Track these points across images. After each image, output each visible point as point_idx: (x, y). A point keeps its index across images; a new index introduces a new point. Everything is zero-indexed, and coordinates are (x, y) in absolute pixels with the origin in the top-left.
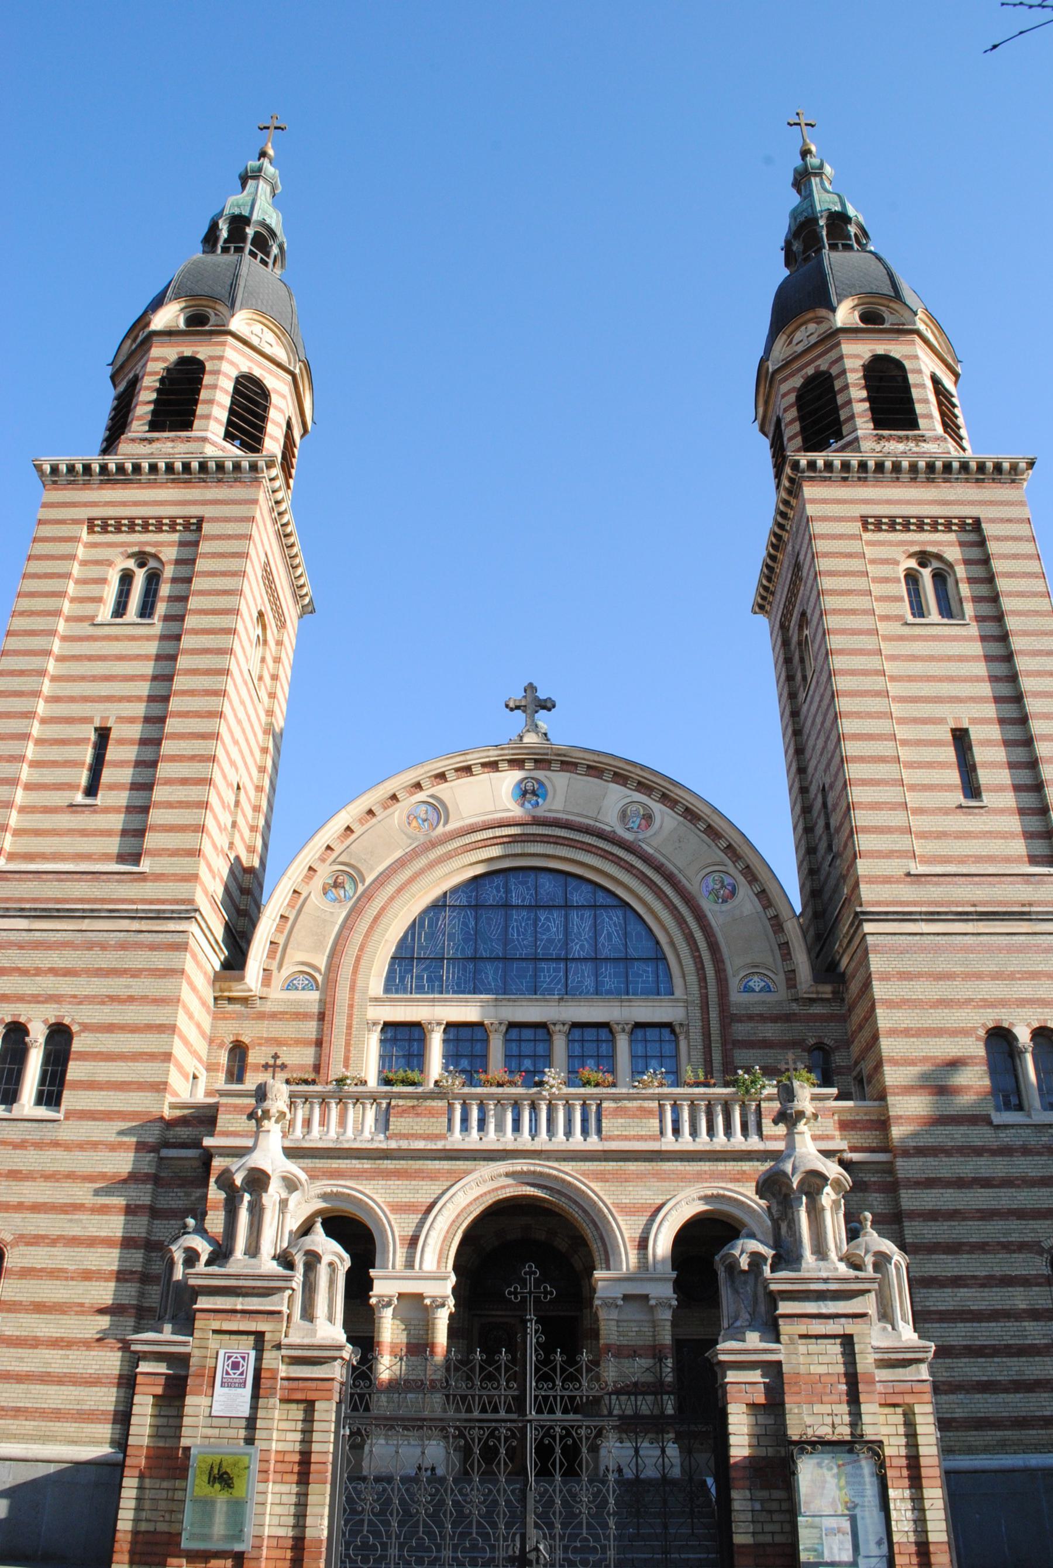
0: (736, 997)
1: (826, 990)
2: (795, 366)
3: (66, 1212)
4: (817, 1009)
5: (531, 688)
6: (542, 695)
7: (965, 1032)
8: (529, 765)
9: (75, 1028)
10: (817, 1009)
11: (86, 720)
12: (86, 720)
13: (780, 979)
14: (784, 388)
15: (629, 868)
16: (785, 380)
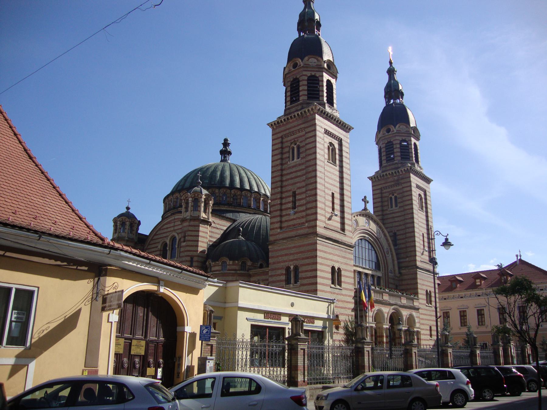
0: (390, 274)
1: (398, 275)
2: (400, 134)
3: (345, 309)
4: (397, 278)
5: (365, 197)
6: (367, 199)
7: (424, 290)
8: (367, 216)
9: (341, 269)
10: (397, 278)
11: (330, 190)
12: (330, 190)
13: (393, 271)
14: (397, 138)
15: (377, 244)
16: (398, 136)
